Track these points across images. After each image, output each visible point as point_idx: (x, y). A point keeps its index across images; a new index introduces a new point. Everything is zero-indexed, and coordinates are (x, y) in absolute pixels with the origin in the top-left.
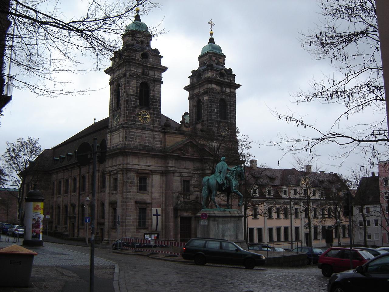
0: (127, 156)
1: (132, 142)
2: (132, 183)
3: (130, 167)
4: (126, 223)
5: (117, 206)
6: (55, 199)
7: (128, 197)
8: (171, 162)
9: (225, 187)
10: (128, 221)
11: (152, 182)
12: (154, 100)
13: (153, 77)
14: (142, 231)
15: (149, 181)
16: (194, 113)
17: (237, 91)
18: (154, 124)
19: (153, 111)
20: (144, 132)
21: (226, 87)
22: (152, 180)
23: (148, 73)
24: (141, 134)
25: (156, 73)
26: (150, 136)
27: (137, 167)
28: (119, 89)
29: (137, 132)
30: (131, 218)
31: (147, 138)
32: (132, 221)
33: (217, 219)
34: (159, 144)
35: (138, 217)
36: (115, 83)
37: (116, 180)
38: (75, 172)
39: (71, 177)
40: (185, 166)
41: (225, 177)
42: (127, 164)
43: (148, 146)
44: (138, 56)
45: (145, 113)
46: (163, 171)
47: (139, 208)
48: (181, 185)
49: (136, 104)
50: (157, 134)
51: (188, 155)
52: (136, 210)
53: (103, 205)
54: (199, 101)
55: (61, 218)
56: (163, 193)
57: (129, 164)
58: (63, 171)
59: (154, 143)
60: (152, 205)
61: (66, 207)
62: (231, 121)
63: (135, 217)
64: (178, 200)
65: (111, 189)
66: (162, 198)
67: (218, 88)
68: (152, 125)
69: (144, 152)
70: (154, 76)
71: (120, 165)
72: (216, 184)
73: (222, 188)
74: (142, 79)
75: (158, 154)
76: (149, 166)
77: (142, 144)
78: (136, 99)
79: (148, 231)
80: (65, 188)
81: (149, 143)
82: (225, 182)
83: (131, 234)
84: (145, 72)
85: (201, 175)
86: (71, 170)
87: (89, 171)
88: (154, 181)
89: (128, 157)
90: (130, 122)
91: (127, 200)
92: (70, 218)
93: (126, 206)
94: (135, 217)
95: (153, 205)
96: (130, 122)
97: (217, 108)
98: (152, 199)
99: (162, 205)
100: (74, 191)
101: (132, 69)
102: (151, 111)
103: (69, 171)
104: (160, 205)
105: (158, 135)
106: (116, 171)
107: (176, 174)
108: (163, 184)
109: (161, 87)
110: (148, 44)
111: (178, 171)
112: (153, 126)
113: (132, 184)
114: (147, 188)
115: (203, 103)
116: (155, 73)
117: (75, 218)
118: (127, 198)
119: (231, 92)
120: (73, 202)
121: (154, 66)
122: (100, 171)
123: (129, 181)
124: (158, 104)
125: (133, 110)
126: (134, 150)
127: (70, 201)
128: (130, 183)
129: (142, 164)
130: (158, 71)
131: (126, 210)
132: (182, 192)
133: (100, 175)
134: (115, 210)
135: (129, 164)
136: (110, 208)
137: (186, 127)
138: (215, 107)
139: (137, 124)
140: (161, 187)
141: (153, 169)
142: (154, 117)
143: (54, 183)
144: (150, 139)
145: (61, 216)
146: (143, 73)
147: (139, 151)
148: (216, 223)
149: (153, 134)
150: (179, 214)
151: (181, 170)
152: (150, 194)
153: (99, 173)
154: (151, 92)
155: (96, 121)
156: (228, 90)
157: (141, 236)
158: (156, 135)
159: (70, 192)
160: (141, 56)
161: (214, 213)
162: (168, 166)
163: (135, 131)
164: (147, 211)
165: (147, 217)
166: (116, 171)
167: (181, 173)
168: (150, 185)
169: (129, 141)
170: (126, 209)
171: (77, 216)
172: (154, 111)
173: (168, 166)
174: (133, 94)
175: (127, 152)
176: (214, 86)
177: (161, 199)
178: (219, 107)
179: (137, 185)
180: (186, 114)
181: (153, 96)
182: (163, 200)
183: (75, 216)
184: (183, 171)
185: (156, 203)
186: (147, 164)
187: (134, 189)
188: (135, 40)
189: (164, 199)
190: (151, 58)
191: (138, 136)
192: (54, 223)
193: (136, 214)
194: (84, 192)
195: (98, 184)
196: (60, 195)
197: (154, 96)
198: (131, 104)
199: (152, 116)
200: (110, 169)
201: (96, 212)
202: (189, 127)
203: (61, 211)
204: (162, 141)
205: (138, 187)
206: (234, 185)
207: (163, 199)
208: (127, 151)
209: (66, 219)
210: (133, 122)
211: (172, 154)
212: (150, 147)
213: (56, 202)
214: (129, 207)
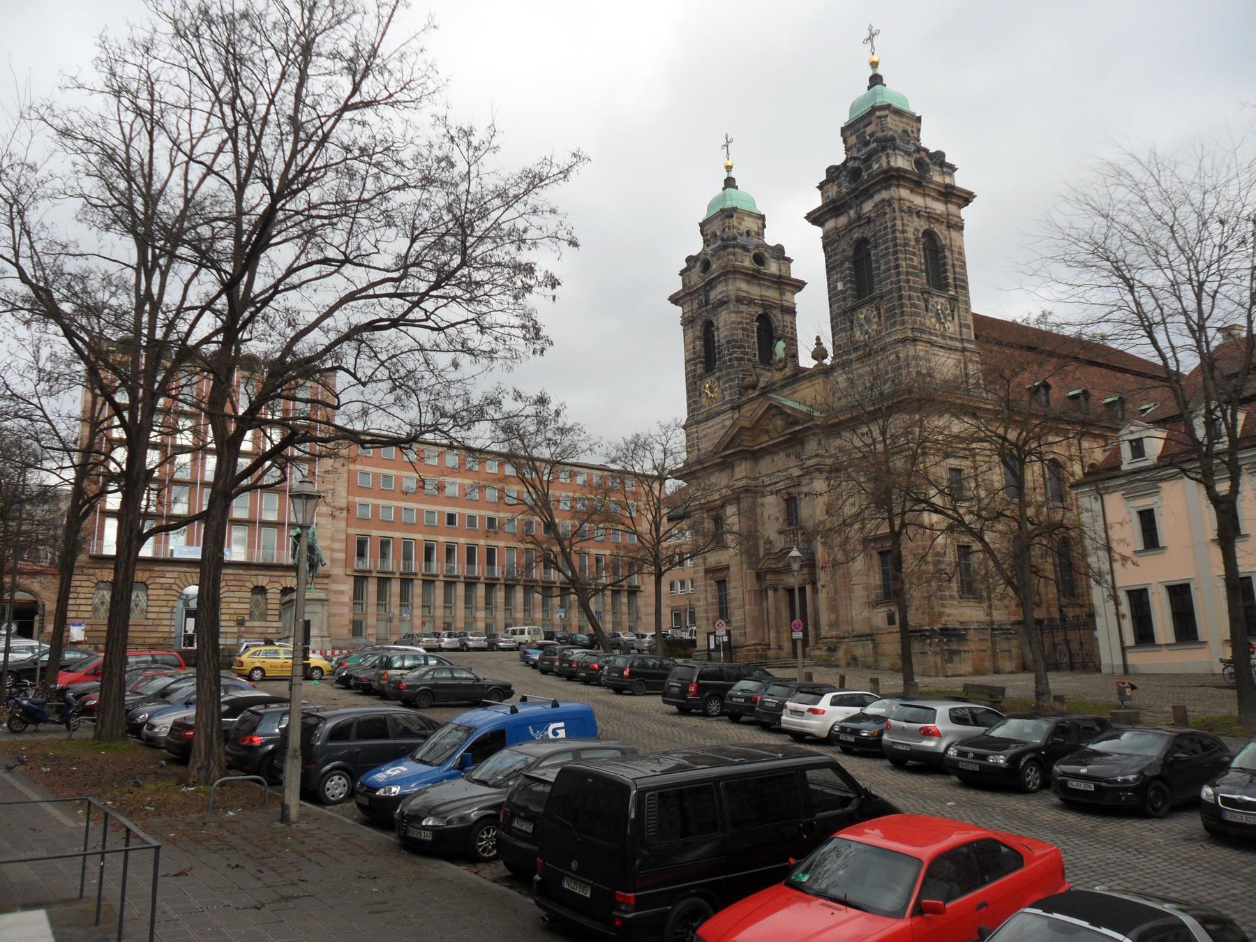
63: (710, 600)
94: (710, 600)
97: (842, 279)
102: (717, 374)
130: (721, 282)
156: (868, 207)
197: (719, 341)
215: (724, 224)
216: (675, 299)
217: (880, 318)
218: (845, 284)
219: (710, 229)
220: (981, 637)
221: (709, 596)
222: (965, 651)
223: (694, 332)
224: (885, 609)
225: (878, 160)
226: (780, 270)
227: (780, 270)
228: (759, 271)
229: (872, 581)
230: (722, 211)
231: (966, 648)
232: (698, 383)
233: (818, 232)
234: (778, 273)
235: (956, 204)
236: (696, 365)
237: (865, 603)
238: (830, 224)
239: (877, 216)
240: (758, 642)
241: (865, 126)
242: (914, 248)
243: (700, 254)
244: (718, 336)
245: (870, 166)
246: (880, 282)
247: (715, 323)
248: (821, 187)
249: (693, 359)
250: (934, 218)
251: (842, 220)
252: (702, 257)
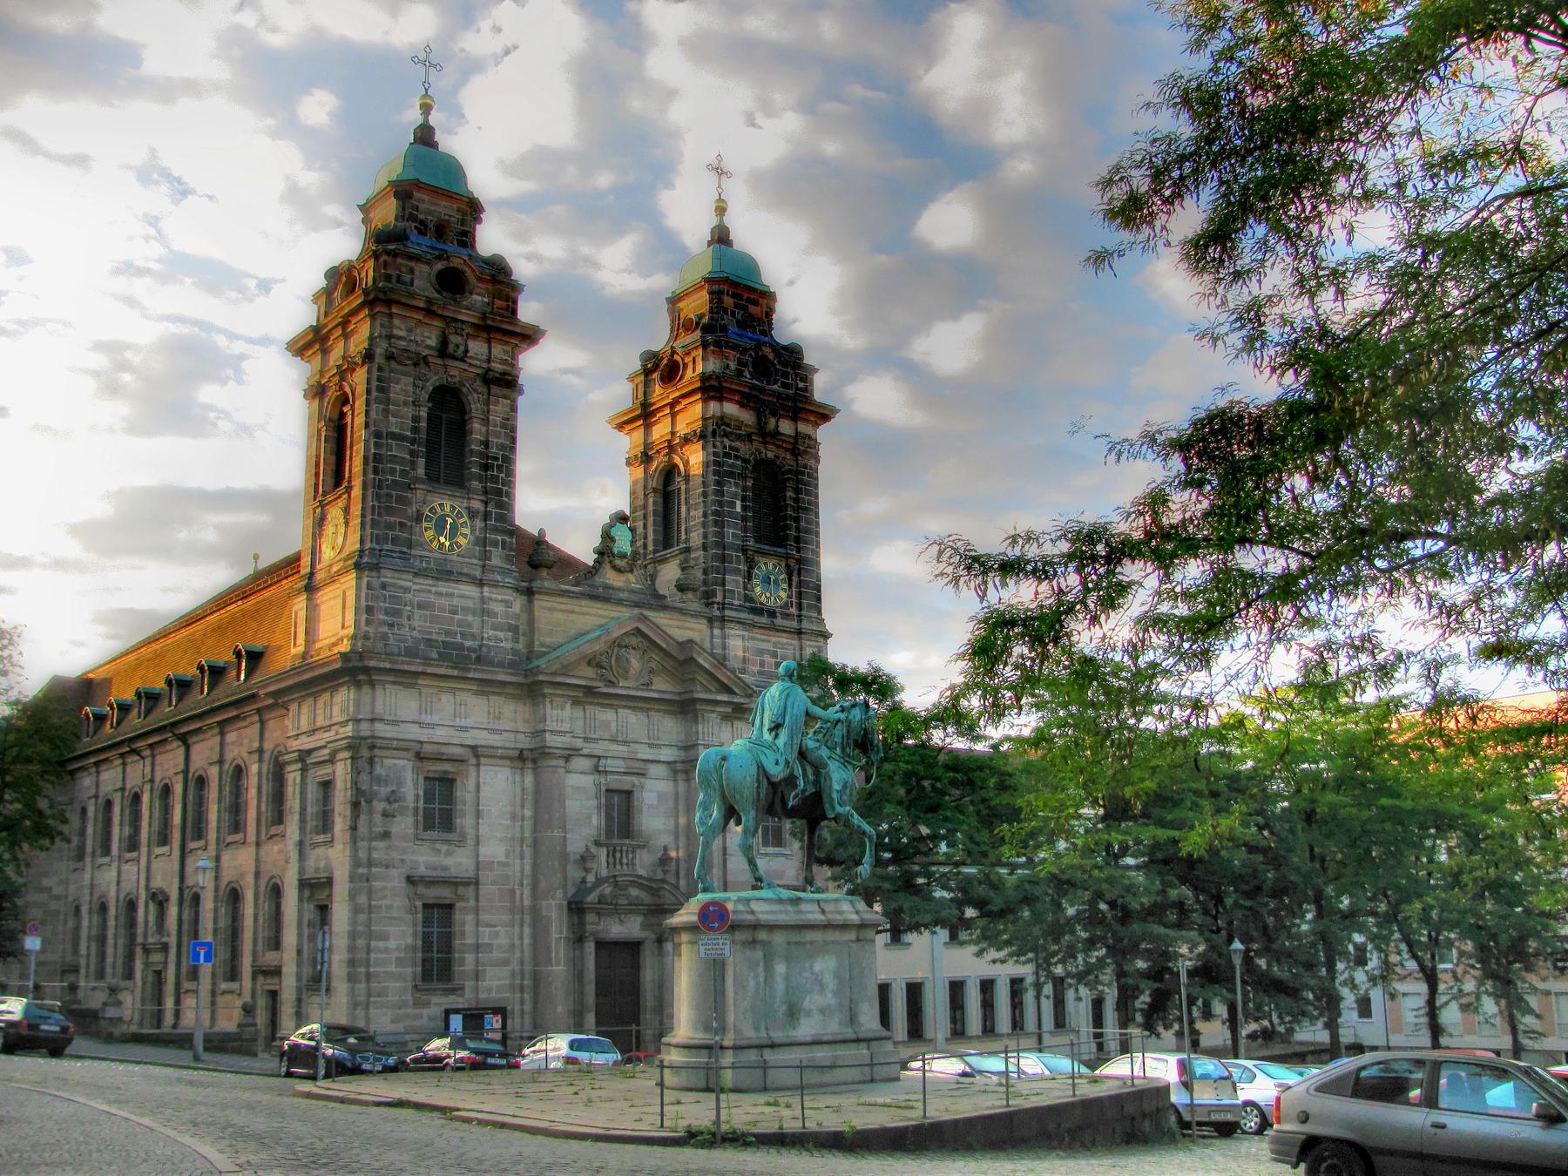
0: (372, 684)
1: (396, 631)
2: (396, 801)
3: (382, 730)
4: (368, 964)
5: (330, 896)
6: (87, 876)
7: (375, 855)
8: (555, 712)
9: (797, 795)
10: (380, 956)
11: (478, 798)
12: (488, 457)
13: (485, 365)
14: (435, 1000)
15: (464, 792)
16: (651, 519)
17: (823, 433)
18: (485, 556)
19: (482, 501)
20: (444, 590)
21: (781, 416)
22: (478, 786)
23: (462, 348)
24: (432, 598)
25: (498, 351)
26: (470, 604)
27: (414, 733)
28: (342, 415)
29: (417, 589)
30: (392, 944)
31: (455, 613)
32: (394, 956)
33: (763, 935)
34: (506, 640)
35: (419, 942)
36: (332, 394)
37: (327, 785)
38: (170, 761)
39: (152, 781)
40: (613, 729)
41: (796, 748)
42: (372, 720)
43: (461, 647)
44: (422, 280)
45: (448, 509)
46: (522, 751)
47: (425, 906)
48: (599, 808)
49: (413, 473)
50: (500, 597)
51: (625, 687)
52: (412, 910)
53: (276, 892)
54: (669, 473)
55: (110, 951)
56: (522, 840)
57: (381, 720)
58: (119, 762)
59: (485, 635)
60: (477, 891)
61: (131, 905)
62: (798, 551)
63: (410, 940)
64: (587, 870)
65: (310, 824)
66: (518, 862)
67: (747, 417)
68: (475, 561)
69: (442, 671)
70: (489, 361)
71: (344, 724)
72: (758, 781)
73: (784, 801)
74: (436, 373)
75: (501, 677)
76: (464, 729)
77: (434, 637)
78: (412, 453)
79: (460, 1000)
80: (127, 831)
81: (463, 635)
82: (798, 771)
83: (389, 1012)
84: (451, 348)
85: (679, 766)
86: (153, 756)
87: (222, 754)
88: (485, 791)
89: (379, 692)
90: (385, 547)
91: (373, 870)
92: (147, 951)
93: (370, 893)
94: (410, 940)
95: (481, 892)
96: (385, 547)
97: (744, 499)
98: (478, 864)
99: (518, 892)
100: (164, 840)
101: (396, 332)
103: (143, 758)
104: (513, 892)
105: (506, 602)
106: (326, 751)
107: (579, 763)
108: (523, 807)
109: (514, 409)
110: (466, 239)
111: (585, 751)
112: (484, 566)
113: (396, 805)
114: (458, 820)
115: (687, 478)
116: (490, 352)
117: (165, 948)
118: (370, 863)
119: (798, 436)
120: (158, 882)
121: (489, 322)
122: (266, 756)
123: (384, 791)
124: (502, 475)
125: (400, 500)
126: (403, 663)
127: (148, 879)
128: (388, 800)
129: (435, 719)
130: (506, 343)
131: (370, 913)
132: (603, 838)
133: (265, 769)
134: (324, 910)
135: (381, 720)
136: (306, 905)
137: (619, 570)
138: (735, 495)
139: (415, 556)
140: (513, 817)
141: (483, 743)
142: (485, 529)
143: (84, 811)
144: (470, 618)
145: (110, 941)
146: (443, 350)
147: (424, 664)
148: (759, 954)
149: (483, 600)
150: (590, 928)
151: (598, 748)
152: (470, 842)
153: (261, 760)
154: (476, 426)
155: (264, 564)
156: (786, 427)
157: (431, 1019)
158: (496, 600)
159: (149, 846)
160: (434, 281)
161: (753, 912)
162: (544, 731)
163: (409, 584)
164: (457, 916)
165: (457, 942)
166: (326, 751)
167: (599, 757)
168: (469, 808)
169: (384, 623)
170: (370, 906)
171: (173, 941)
172: (486, 503)
173: (544, 731)
174: (400, 434)
175: (375, 669)
176: (731, 409)
177: (518, 868)
178: (749, 494)
179: (416, 809)
180: (622, 518)
181: (482, 443)
182: (522, 871)
183: (164, 940)
184: (606, 750)
185: (494, 883)
186: (458, 723)
187: (404, 825)
188: (412, 218)
189: (528, 868)
190: (478, 290)
191: (421, 606)
192: (83, 971)
193: (410, 931)
194: (202, 843)
195: (259, 808)
196: (107, 859)
197: (486, 444)
198: (393, 471)
199: (479, 523)
200: (305, 743)
201: (248, 922)
202: (631, 571)
203: (111, 923)
204: (517, 627)
205: (420, 818)
206: (836, 786)
207: (522, 865)
208: (372, 663)
209: (130, 957)
210: (398, 549)
211: (559, 679)
212: (469, 649)
213: (92, 886)
214: (384, 898)
217: (790, 586)
218: (744, 508)
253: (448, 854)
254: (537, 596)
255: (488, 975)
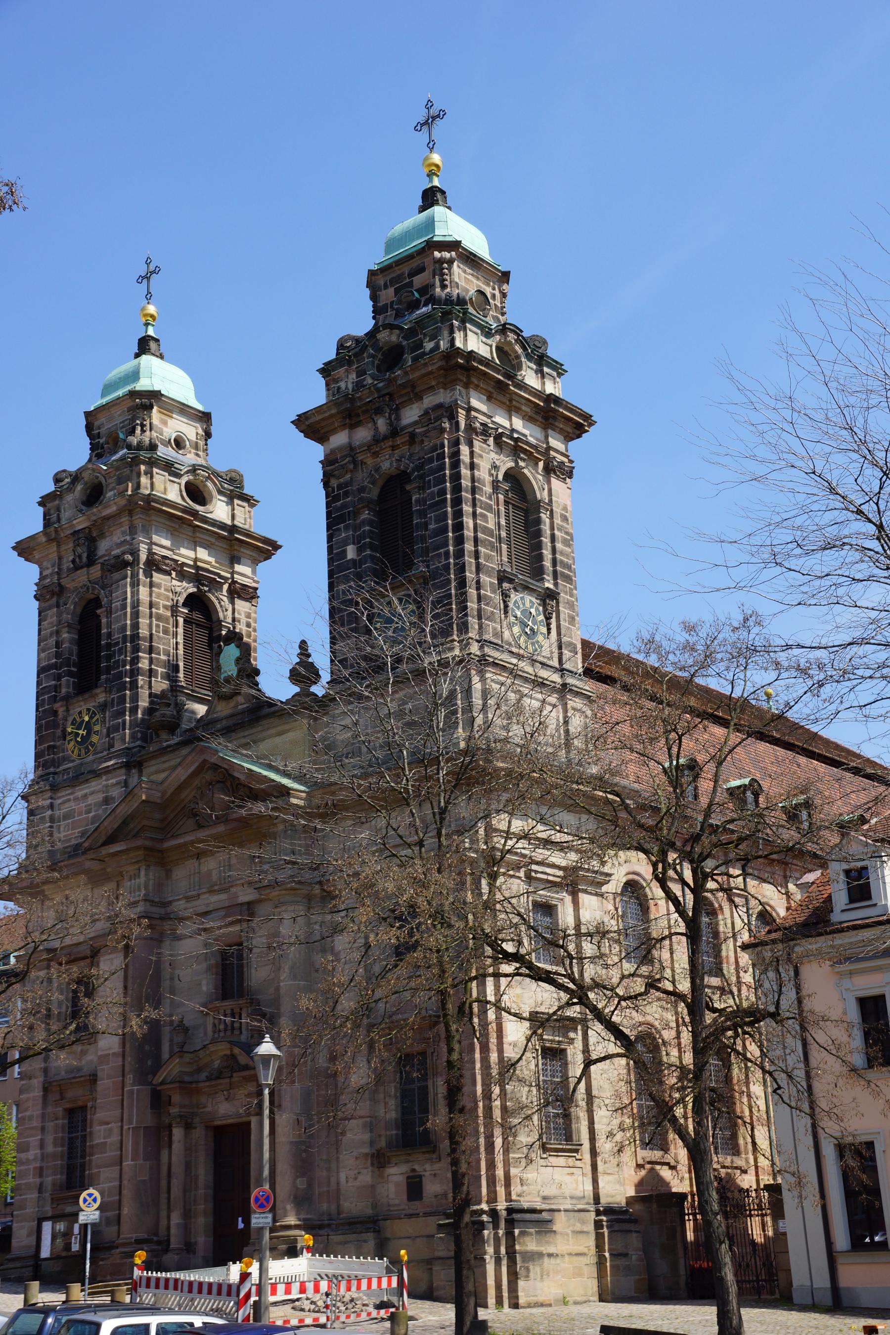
23: (85, 555)
32: (31, 1167)
63: (50, 1149)
78: (59, 678)
94: (50, 1149)
97: (356, 541)
184: (207, 905)
197: (109, 635)
214: (26, 1110)
215: (133, 419)
216: (24, 549)
218: (360, 550)
219: (105, 425)
220: (578, 1227)
221: (49, 1138)
222: (550, 1255)
223: (59, 615)
224: (404, 1168)
225: (434, 337)
226: (233, 517)
227: (233, 517)
228: (195, 514)
229: (381, 1112)
230: (133, 394)
231: (552, 1249)
232: (61, 711)
233: (316, 451)
234: (229, 522)
235: (561, 431)
236: (59, 678)
237: (366, 1155)
238: (340, 439)
239: (426, 432)
240: (146, 1236)
241: (412, 274)
242: (490, 498)
243: (81, 470)
244: (109, 625)
245: (420, 345)
246: (426, 552)
247: (105, 601)
248: (326, 371)
249: (55, 666)
250: (525, 451)
251: (363, 434)
252: (86, 475)
253: (84, 1053)
254: (145, 764)
255: (102, 1177)
